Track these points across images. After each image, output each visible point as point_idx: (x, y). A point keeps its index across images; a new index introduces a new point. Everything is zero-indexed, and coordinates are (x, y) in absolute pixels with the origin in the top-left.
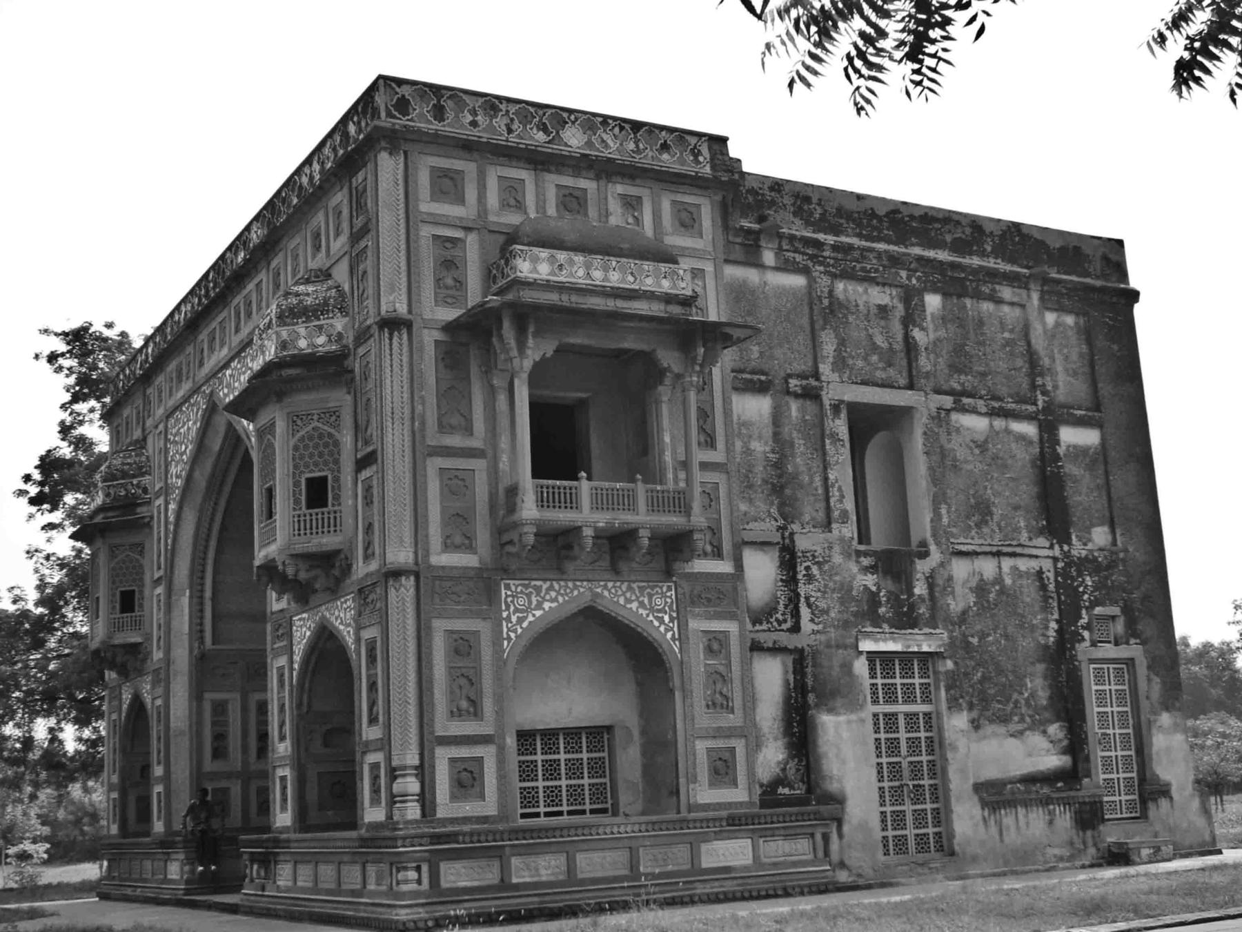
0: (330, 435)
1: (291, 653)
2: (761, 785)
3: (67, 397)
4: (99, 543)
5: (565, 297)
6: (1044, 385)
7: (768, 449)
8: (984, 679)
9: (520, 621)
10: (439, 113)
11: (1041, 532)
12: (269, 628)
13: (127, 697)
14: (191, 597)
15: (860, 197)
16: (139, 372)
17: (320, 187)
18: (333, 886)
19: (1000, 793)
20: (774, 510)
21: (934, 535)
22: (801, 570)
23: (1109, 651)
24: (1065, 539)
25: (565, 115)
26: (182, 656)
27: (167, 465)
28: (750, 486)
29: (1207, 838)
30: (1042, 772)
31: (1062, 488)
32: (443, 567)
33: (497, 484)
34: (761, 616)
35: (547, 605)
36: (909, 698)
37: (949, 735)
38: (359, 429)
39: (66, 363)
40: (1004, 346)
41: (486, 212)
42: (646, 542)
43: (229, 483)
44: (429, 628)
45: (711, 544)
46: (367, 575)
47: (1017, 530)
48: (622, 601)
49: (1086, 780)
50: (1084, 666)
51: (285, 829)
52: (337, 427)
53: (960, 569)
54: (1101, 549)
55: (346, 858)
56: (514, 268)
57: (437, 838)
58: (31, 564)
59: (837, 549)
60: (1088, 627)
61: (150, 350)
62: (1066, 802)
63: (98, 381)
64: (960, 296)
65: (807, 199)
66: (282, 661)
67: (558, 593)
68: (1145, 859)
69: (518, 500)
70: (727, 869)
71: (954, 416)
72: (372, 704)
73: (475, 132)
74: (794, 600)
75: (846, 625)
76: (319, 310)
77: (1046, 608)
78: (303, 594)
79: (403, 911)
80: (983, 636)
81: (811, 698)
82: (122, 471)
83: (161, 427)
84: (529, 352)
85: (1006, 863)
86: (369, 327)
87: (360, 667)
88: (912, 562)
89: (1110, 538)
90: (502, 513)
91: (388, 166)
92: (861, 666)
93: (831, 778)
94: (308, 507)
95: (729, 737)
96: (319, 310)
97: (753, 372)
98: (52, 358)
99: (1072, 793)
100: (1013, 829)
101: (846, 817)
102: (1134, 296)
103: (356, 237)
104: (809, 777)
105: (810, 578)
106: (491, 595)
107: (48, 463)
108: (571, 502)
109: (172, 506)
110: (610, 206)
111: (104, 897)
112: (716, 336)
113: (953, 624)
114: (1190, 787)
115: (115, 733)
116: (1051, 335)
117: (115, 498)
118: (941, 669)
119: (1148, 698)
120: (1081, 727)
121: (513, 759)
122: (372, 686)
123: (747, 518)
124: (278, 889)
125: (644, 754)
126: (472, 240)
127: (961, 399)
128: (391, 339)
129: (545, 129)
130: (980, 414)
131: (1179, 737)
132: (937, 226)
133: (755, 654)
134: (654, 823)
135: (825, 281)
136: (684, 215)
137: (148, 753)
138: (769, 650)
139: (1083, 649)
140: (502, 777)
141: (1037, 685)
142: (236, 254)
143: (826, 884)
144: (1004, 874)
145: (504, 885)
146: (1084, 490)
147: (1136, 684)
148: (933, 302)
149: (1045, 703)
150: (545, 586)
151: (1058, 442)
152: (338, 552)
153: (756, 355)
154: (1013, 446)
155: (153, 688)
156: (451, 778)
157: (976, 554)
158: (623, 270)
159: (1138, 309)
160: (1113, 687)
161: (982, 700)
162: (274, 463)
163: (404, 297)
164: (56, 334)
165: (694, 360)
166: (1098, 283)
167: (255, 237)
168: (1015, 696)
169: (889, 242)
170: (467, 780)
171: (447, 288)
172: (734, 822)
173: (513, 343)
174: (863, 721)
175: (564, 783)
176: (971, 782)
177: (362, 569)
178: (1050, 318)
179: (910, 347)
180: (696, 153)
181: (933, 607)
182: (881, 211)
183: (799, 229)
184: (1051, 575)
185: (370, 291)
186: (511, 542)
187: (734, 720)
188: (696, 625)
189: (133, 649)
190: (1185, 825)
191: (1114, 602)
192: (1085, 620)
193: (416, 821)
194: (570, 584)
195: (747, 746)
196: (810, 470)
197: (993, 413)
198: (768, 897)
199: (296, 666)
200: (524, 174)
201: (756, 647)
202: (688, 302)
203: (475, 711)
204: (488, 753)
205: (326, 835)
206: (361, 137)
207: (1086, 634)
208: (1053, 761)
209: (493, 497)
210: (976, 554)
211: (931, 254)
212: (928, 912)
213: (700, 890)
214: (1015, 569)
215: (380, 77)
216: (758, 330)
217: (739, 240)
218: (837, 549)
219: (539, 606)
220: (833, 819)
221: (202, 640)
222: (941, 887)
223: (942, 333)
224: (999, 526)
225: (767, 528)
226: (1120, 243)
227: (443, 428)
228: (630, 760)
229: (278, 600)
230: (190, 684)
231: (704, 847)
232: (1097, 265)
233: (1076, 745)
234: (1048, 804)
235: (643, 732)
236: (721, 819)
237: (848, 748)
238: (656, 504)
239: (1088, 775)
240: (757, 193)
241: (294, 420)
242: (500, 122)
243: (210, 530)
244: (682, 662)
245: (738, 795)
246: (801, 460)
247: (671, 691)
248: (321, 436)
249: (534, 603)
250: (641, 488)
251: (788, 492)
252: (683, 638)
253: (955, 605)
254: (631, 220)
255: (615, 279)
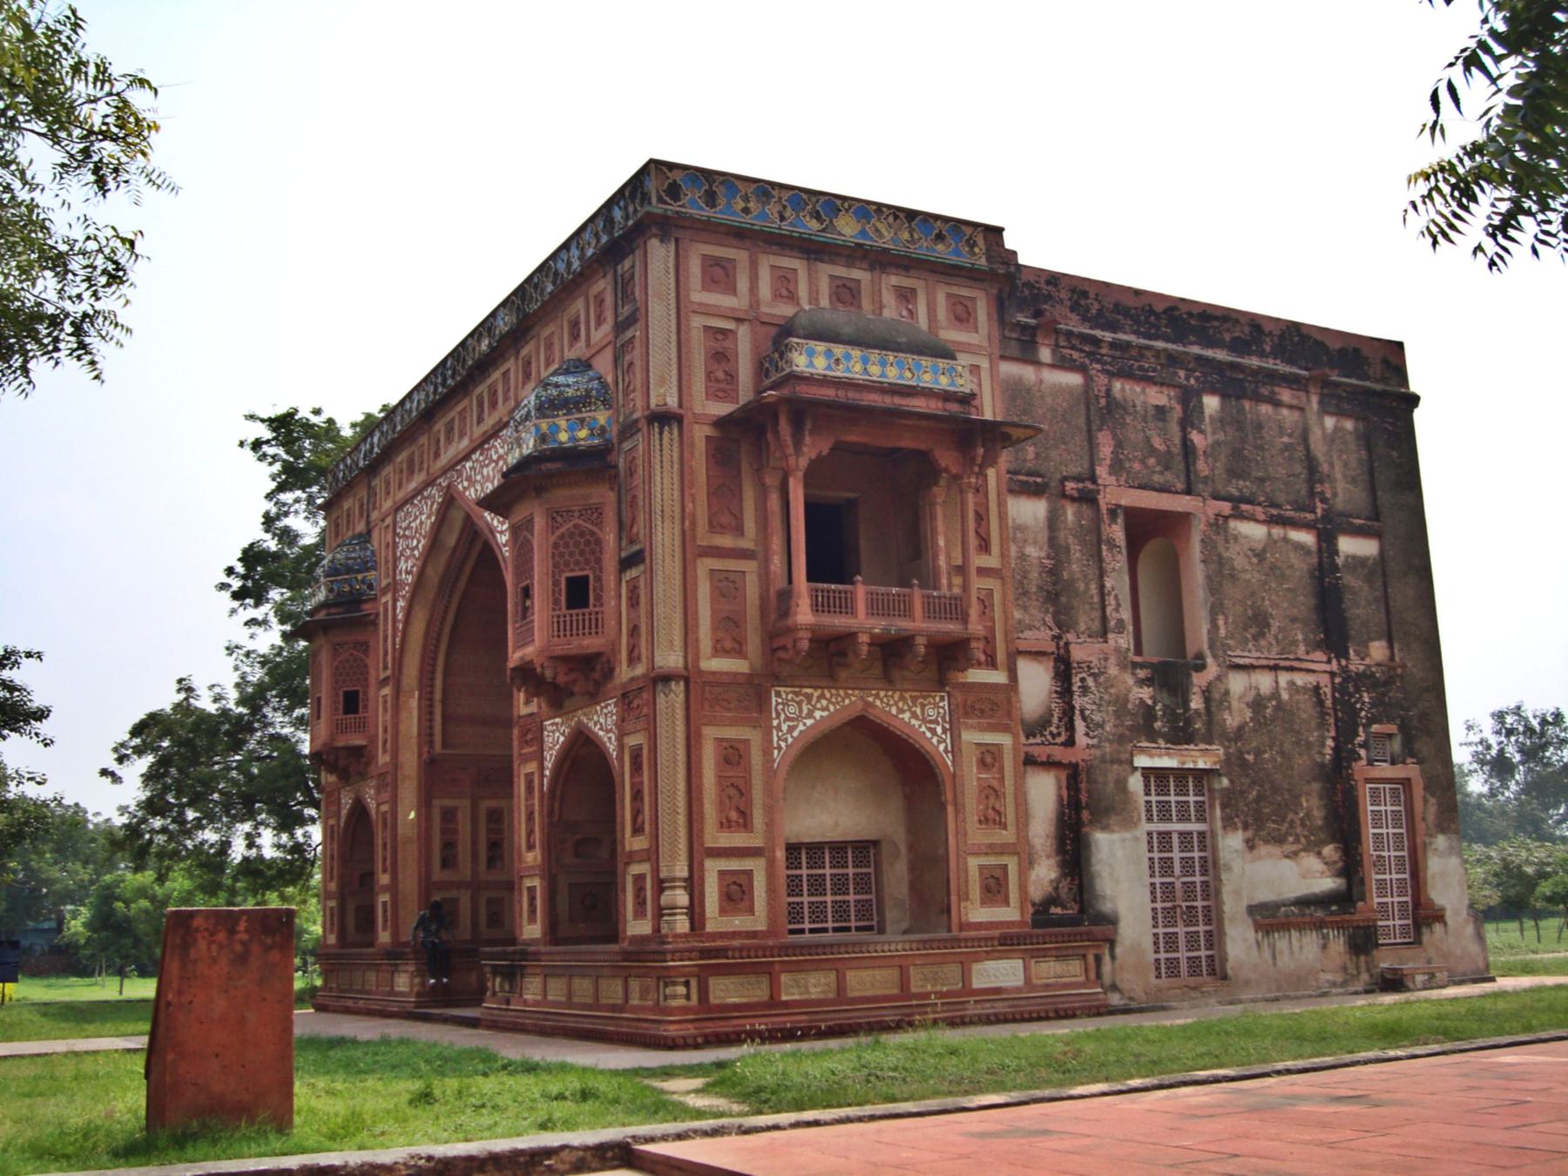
0: (593, 533)
1: (542, 760)
2: (1034, 904)
3: (274, 485)
4: (321, 640)
5: (841, 393)
6: (1323, 493)
7: (1043, 554)
8: (1260, 798)
9: (791, 729)
10: (711, 199)
11: (1318, 646)
12: (516, 732)
13: (347, 801)
14: (420, 698)
15: (1138, 293)
16: (361, 464)
17: (581, 274)
18: (589, 1001)
19: (1274, 916)
20: (1049, 618)
21: (1211, 647)
22: (1076, 680)
23: (1384, 770)
24: (1342, 653)
25: (839, 202)
26: (410, 761)
27: (396, 561)
28: (1025, 593)
29: (1481, 965)
30: (1315, 895)
31: (1340, 600)
32: (713, 673)
33: (768, 584)
34: (1035, 728)
35: (818, 714)
36: (1184, 817)
37: (1224, 856)
38: (624, 528)
39: (270, 450)
40: (1282, 451)
41: (758, 302)
42: (922, 650)
43: (470, 583)
44: (699, 735)
45: (985, 652)
46: (632, 679)
47: (1294, 643)
48: (894, 711)
49: (1360, 904)
50: (1360, 784)
51: (534, 942)
52: (599, 524)
53: (1237, 684)
54: (1378, 665)
55: (606, 972)
56: (790, 362)
57: (706, 953)
58: (231, 661)
59: (1112, 660)
60: (1365, 745)
61: (376, 440)
62: (1339, 926)
63: (306, 470)
64: (1238, 398)
65: (1085, 294)
66: (531, 767)
67: (829, 701)
68: (1420, 986)
69: (793, 604)
70: (998, 990)
71: (1232, 524)
72: (637, 813)
73: (748, 219)
74: (1068, 713)
75: (1121, 739)
76: (583, 402)
77: (1322, 725)
78: (558, 698)
79: (672, 1027)
80: (1258, 753)
81: (1085, 815)
82: (346, 566)
83: (389, 520)
84: (805, 449)
85: (1279, 988)
86: (636, 421)
87: (623, 774)
88: (1189, 676)
89: (1387, 652)
90: (773, 617)
91: (659, 255)
92: (1135, 783)
93: (1104, 897)
94: (569, 607)
95: (1002, 854)
96: (583, 402)
97: (1029, 474)
98: (257, 445)
99: (1347, 917)
100: (1286, 952)
101: (1119, 939)
102: (1414, 400)
103: (620, 327)
104: (1081, 896)
105: (1085, 690)
106: (762, 703)
107: (252, 556)
108: (847, 607)
109: (401, 603)
110: (883, 299)
111: (321, 1008)
112: (996, 435)
113: (1229, 740)
114: (1464, 912)
115: (332, 839)
116: (1330, 440)
117: (338, 594)
118: (1217, 786)
119: (1424, 819)
120: (1356, 849)
121: (782, 872)
122: (637, 795)
123: (1022, 626)
124: (525, 1002)
125: (912, 869)
126: (743, 332)
127: (1240, 506)
128: (661, 433)
129: (818, 217)
130: (1257, 521)
131: (1454, 861)
132: (1216, 324)
133: (1029, 769)
134: (925, 942)
135: (1102, 380)
136: (959, 308)
137: (372, 860)
138: (1042, 764)
139: (1359, 767)
140: (771, 891)
141: (1312, 805)
142: (479, 341)
143: (1098, 1007)
144: (1276, 999)
145: (774, 1003)
146: (1363, 603)
147: (1412, 807)
148: (1211, 403)
149: (1320, 823)
150: (817, 693)
151: (1336, 552)
152: (598, 655)
153: (1031, 456)
154: (1292, 555)
155: (378, 790)
156: (720, 892)
157: (1253, 667)
158: (900, 365)
159: (1419, 415)
160: (1389, 808)
161: (1256, 820)
162: (532, 558)
163: (675, 390)
164: (263, 421)
165: (973, 461)
166: (1379, 387)
167: (502, 325)
168: (1291, 816)
169: (1167, 340)
170: (736, 893)
171: (717, 380)
172: (1006, 942)
173: (789, 441)
174: (1137, 839)
175: (829, 898)
176: (1245, 903)
177: (625, 673)
178: (1330, 422)
179: (1188, 450)
180: (972, 244)
181: (1210, 723)
182: (1159, 308)
183: (1074, 325)
184: (1328, 690)
185: (638, 382)
186: (784, 648)
187: (1008, 836)
188: (970, 737)
189: (357, 752)
190: (1458, 952)
191: (1390, 720)
192: (1361, 738)
193: (685, 935)
194: (842, 692)
195: (1019, 864)
196: (1085, 576)
197: (1271, 521)
198: (1039, 1019)
199: (547, 773)
200: (796, 264)
201: (1030, 761)
202: (967, 399)
203: (745, 823)
204: (757, 866)
205: (583, 948)
206: (630, 223)
207: (1363, 752)
208: (1328, 883)
209: (764, 599)
210: (1253, 667)
211: (1209, 353)
212: (1218, 1034)
213: (972, 1010)
214: (1292, 684)
215: (651, 161)
216: (1040, 430)
217: (1014, 335)
218: (1112, 660)
219: (810, 715)
220: (1105, 940)
221: (431, 743)
222: (1216, 1011)
223: (1221, 436)
224: (1276, 638)
225: (1041, 637)
226: (1400, 345)
227: (714, 527)
228: (897, 877)
229: (527, 702)
230: (419, 788)
231: (976, 967)
232: (1377, 369)
233: (1351, 867)
234: (1321, 928)
235: (911, 848)
236: (992, 939)
237: (1122, 866)
238: (932, 611)
239: (1363, 899)
240: (1033, 286)
241: (554, 517)
242: (772, 209)
243: (441, 629)
244: (954, 776)
245: (1009, 913)
246: (1077, 565)
247: (943, 806)
248: (582, 534)
249: (805, 711)
250: (917, 594)
251: (1063, 599)
252: (955, 750)
253: (1231, 721)
254: (905, 313)
255: (892, 375)
